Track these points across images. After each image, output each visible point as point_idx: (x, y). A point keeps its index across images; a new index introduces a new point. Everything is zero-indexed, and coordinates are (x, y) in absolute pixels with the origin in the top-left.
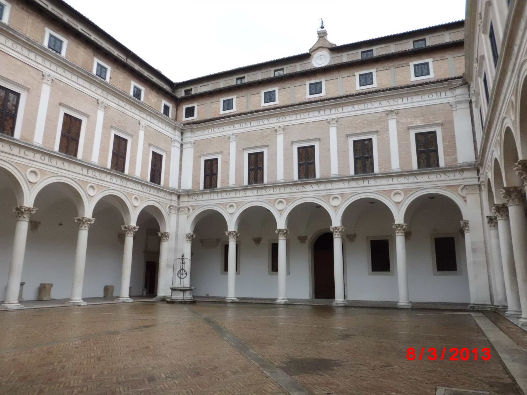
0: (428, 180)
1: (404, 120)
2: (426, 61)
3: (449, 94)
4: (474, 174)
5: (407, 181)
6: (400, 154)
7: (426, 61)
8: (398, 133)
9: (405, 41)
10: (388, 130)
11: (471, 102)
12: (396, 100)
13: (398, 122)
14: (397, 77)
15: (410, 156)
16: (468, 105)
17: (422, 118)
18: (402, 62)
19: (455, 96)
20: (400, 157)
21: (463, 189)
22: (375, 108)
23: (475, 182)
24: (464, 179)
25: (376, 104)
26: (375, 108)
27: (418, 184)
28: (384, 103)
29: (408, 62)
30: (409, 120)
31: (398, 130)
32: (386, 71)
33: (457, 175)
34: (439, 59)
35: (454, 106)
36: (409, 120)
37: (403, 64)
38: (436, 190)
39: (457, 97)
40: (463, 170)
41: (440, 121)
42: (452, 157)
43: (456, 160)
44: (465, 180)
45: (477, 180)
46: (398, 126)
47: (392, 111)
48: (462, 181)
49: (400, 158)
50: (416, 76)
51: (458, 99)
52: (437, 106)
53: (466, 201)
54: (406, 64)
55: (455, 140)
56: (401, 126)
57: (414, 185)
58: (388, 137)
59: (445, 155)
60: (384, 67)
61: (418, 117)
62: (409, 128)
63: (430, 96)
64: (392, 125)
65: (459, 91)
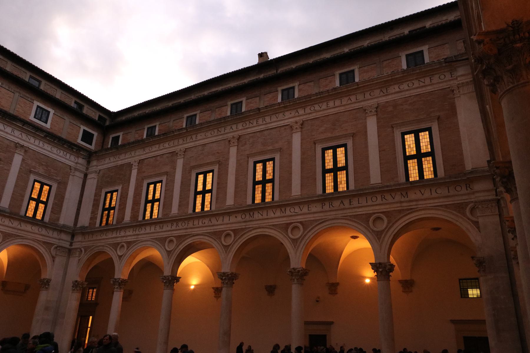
0: (30, 230)
1: (29, 162)
2: (49, 109)
3: (72, 158)
4: (68, 238)
5: (10, 225)
6: (13, 194)
7: (49, 109)
8: (19, 171)
9: (23, 69)
10: (11, 164)
11: (86, 175)
12: (29, 137)
13: (23, 160)
14: (18, 106)
15: (22, 200)
16: (82, 175)
17: (46, 168)
18: (28, 95)
19: (76, 163)
20: (12, 197)
21: (56, 248)
22: (7, 133)
23: (67, 245)
24: (59, 239)
25: (9, 130)
26: (7, 133)
27: (19, 232)
28: (17, 133)
29: (33, 98)
30: (34, 164)
31: (20, 168)
32: (10, 93)
33: (55, 235)
34: (59, 115)
35: (73, 171)
36: (34, 164)
37: (28, 97)
38: (34, 243)
39: (78, 165)
40: (61, 231)
41: (58, 178)
42: (56, 216)
43: (58, 219)
44: (61, 241)
45: (69, 244)
46: (21, 165)
47: (22, 146)
48: (57, 241)
49: (12, 197)
50: (35, 117)
51: (79, 167)
52: (60, 164)
53: (54, 261)
54: (31, 99)
55: (63, 201)
56: (24, 165)
57: (16, 231)
58: (9, 170)
59: (52, 212)
60: (9, 87)
61: (42, 164)
62: (31, 172)
63: (59, 151)
64: (17, 159)
65: (81, 160)
